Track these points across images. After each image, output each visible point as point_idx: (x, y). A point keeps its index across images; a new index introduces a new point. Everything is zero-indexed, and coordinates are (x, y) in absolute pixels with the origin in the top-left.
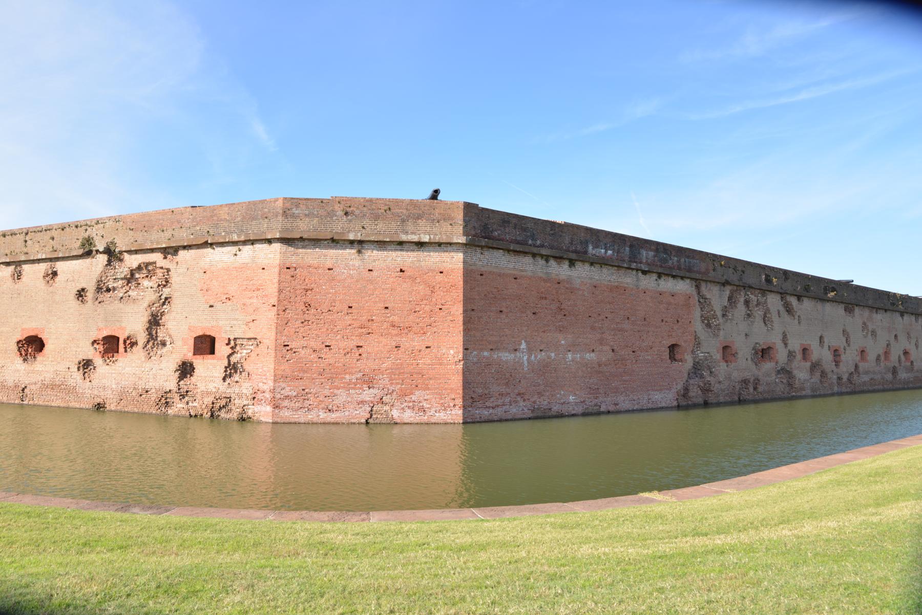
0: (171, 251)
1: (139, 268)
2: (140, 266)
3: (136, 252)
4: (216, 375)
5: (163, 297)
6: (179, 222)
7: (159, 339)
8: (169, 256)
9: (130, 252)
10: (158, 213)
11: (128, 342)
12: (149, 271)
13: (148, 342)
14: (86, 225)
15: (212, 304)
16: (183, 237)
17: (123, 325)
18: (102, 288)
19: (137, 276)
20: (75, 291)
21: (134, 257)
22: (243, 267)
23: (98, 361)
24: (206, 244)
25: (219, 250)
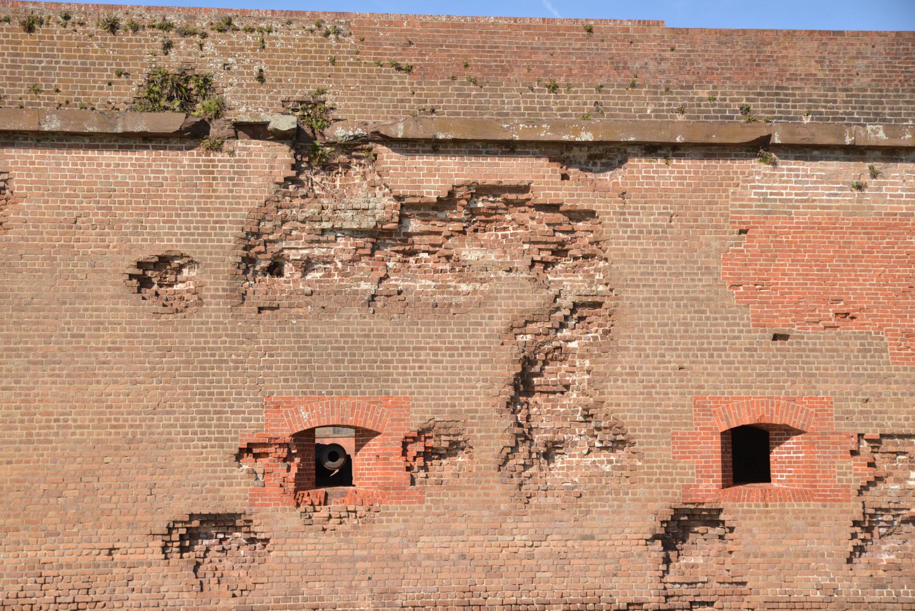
0: (582, 155)
1: (447, 202)
2: (451, 194)
3: (435, 146)
4: (825, 547)
5: (566, 302)
6: (619, 66)
7: (537, 437)
8: (573, 171)
9: (408, 145)
10: (516, 25)
11: (419, 447)
12: (473, 212)
13: (514, 449)
14: (166, 27)
15: (781, 329)
16: (640, 112)
17: (397, 389)
18: (257, 258)
19: (414, 225)
20: (127, 265)
21: (422, 161)
22: (893, 226)
23: (278, 516)
24: (759, 147)
25: (789, 167)
